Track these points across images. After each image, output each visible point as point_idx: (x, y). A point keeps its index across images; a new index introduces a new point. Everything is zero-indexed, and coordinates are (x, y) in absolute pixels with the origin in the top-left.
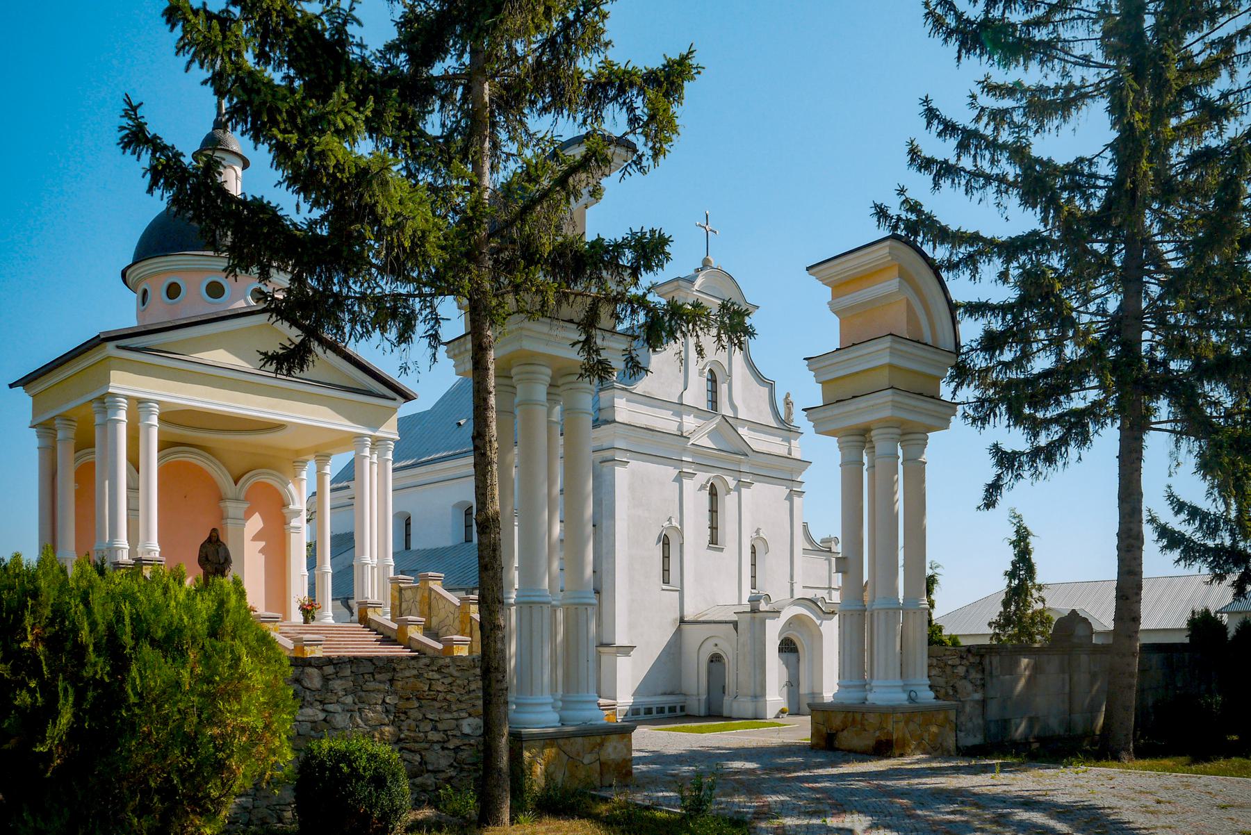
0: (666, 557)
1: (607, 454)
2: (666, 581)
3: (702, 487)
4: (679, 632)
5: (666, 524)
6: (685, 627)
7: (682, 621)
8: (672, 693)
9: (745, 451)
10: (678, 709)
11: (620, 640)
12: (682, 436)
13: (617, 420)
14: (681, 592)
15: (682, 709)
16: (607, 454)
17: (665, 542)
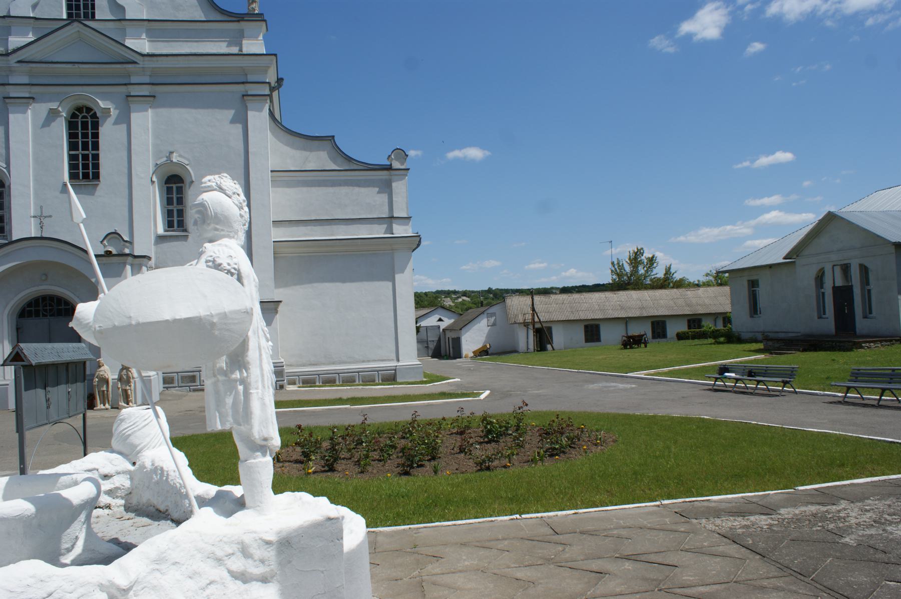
3: (53, 114)
9: (131, 59)
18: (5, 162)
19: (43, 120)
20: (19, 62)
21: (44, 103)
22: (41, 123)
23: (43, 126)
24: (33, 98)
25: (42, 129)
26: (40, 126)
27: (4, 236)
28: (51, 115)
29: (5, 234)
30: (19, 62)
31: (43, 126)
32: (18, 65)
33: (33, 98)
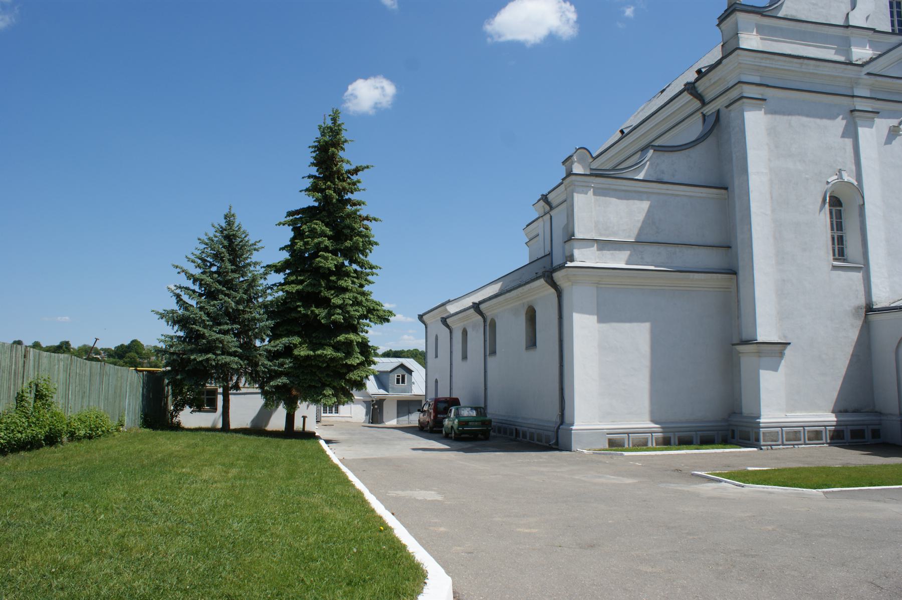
0: (838, 224)
1: (734, 94)
2: (840, 252)
4: (866, 329)
5: (833, 179)
6: (874, 317)
7: (869, 309)
8: (856, 411)
10: (868, 434)
11: (766, 332)
12: (851, 64)
13: (743, 45)
14: (865, 268)
15: (876, 433)
16: (734, 94)
17: (835, 202)
18: (855, 178)
19: (885, 137)
20: (869, 74)
21: (885, 118)
22: (884, 141)
23: (886, 143)
24: (878, 113)
25: (885, 146)
26: (883, 144)
27: (844, 259)
28: (892, 133)
29: (845, 258)
30: (869, 74)
31: (886, 143)
32: (867, 77)
33: (878, 113)
